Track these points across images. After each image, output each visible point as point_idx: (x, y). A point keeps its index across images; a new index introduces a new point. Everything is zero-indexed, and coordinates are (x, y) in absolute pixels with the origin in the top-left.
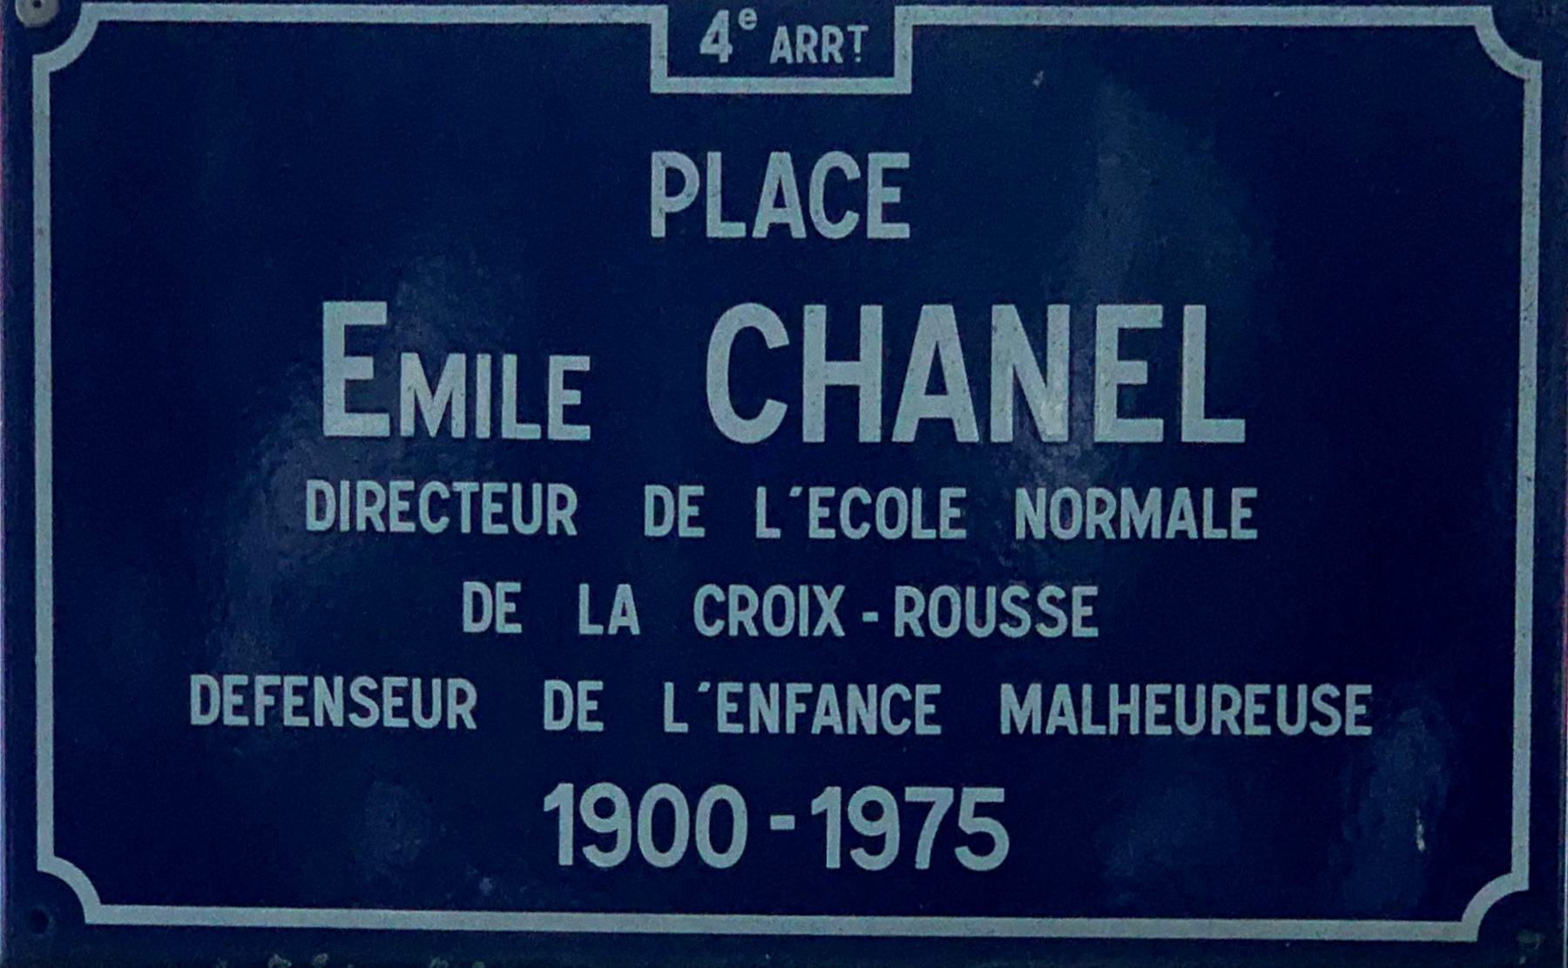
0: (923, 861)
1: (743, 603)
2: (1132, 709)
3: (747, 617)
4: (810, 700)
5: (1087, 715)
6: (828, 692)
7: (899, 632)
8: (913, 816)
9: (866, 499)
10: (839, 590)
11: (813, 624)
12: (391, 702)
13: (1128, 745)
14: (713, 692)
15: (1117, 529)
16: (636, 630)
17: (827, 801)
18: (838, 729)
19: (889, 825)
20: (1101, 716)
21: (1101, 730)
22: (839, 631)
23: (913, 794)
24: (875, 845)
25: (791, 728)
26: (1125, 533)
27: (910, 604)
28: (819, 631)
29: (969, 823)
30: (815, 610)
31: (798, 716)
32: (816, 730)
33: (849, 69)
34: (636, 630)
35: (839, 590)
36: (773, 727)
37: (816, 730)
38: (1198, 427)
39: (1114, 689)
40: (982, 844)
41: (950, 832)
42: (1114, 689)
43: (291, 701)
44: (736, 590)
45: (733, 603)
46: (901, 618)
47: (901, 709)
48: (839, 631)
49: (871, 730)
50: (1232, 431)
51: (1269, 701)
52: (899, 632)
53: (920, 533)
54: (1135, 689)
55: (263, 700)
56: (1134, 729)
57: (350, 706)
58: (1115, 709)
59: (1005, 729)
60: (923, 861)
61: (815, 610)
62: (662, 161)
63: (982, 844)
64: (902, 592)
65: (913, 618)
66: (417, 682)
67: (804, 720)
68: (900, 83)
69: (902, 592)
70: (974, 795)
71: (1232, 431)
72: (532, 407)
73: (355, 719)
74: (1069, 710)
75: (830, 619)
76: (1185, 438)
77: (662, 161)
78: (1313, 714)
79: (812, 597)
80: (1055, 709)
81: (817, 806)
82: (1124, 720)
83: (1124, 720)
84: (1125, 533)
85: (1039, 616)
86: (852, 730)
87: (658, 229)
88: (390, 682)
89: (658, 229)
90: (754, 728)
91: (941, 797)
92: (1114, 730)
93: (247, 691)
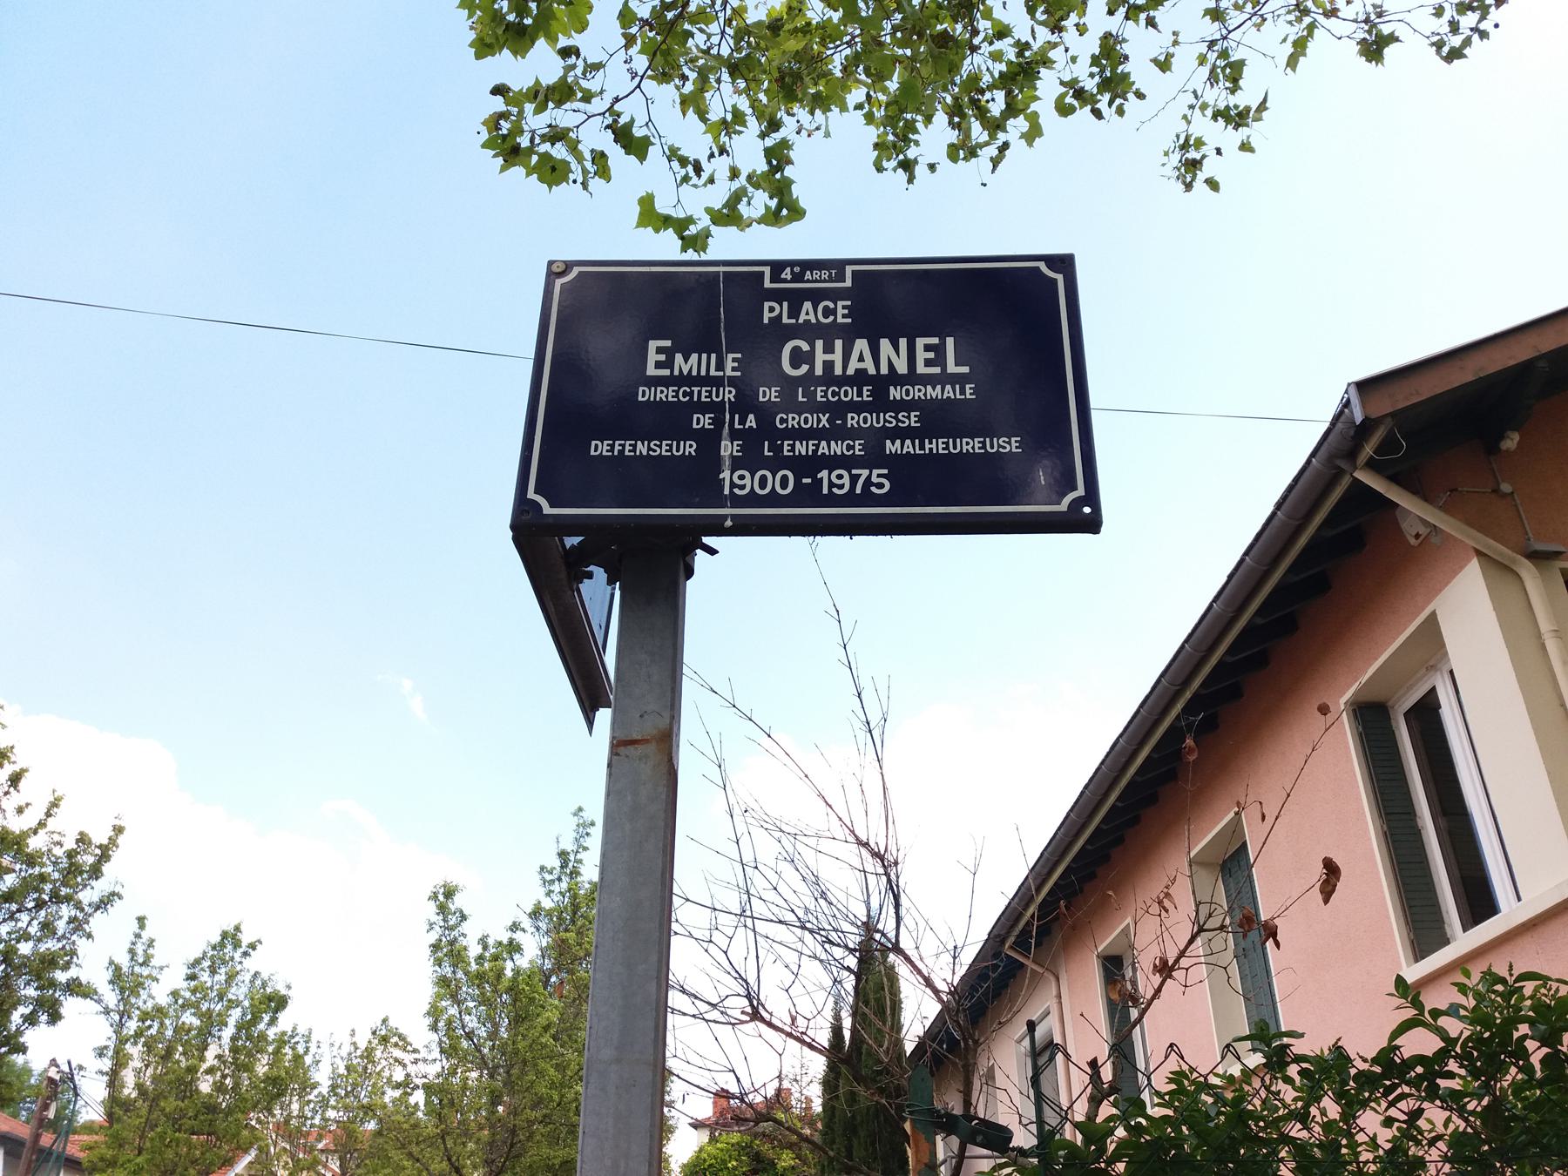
0: (858, 491)
1: (793, 419)
2: (934, 446)
3: (795, 423)
4: (817, 446)
5: (917, 448)
6: (824, 443)
7: (849, 426)
8: (854, 479)
9: (837, 390)
10: (827, 415)
11: (818, 424)
12: (664, 447)
13: (932, 457)
14: (782, 444)
15: (926, 397)
16: (755, 427)
17: (824, 474)
18: (827, 453)
19: (846, 481)
20: (922, 447)
21: (923, 452)
22: (827, 426)
23: (854, 472)
24: (841, 487)
25: (810, 453)
26: (929, 397)
27: (853, 418)
28: (821, 426)
29: (875, 479)
30: (819, 421)
31: (813, 450)
32: (819, 454)
33: (830, 280)
34: (755, 427)
35: (827, 415)
36: (804, 453)
37: (819, 454)
38: (952, 368)
39: (927, 441)
40: (881, 486)
41: (868, 480)
42: (927, 441)
43: (628, 448)
44: (790, 416)
45: (790, 419)
46: (849, 422)
47: (849, 448)
48: (827, 426)
49: (839, 453)
50: (965, 369)
51: (984, 443)
52: (849, 426)
53: (855, 398)
54: (934, 441)
55: (617, 448)
56: (935, 451)
57: (650, 449)
58: (927, 446)
59: (888, 452)
60: (858, 491)
61: (819, 421)
62: (767, 305)
63: (881, 486)
64: (850, 415)
65: (854, 422)
66: (675, 443)
67: (815, 451)
68: (848, 283)
69: (850, 415)
70: (876, 472)
71: (965, 369)
72: (720, 367)
73: (651, 453)
74: (911, 446)
75: (824, 422)
76: (949, 371)
77: (767, 305)
78: (999, 446)
79: (818, 416)
80: (906, 446)
81: (819, 476)
82: (931, 449)
83: (931, 449)
84: (929, 397)
85: (898, 421)
86: (832, 453)
87: (766, 321)
88: (664, 443)
89: (766, 321)
90: (797, 453)
91: (865, 473)
92: (927, 452)
93: (612, 446)
